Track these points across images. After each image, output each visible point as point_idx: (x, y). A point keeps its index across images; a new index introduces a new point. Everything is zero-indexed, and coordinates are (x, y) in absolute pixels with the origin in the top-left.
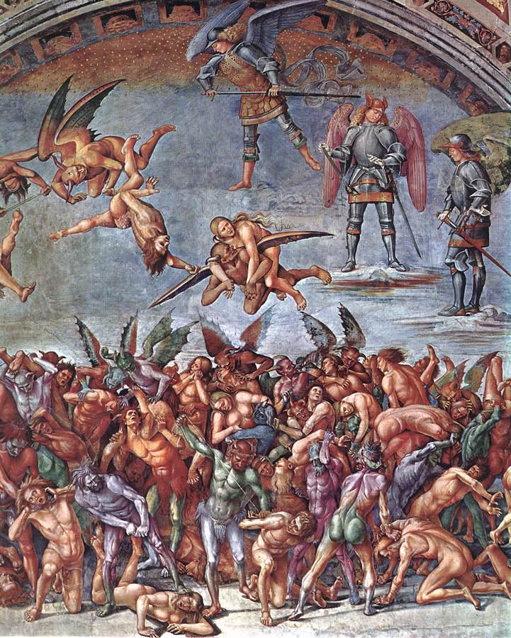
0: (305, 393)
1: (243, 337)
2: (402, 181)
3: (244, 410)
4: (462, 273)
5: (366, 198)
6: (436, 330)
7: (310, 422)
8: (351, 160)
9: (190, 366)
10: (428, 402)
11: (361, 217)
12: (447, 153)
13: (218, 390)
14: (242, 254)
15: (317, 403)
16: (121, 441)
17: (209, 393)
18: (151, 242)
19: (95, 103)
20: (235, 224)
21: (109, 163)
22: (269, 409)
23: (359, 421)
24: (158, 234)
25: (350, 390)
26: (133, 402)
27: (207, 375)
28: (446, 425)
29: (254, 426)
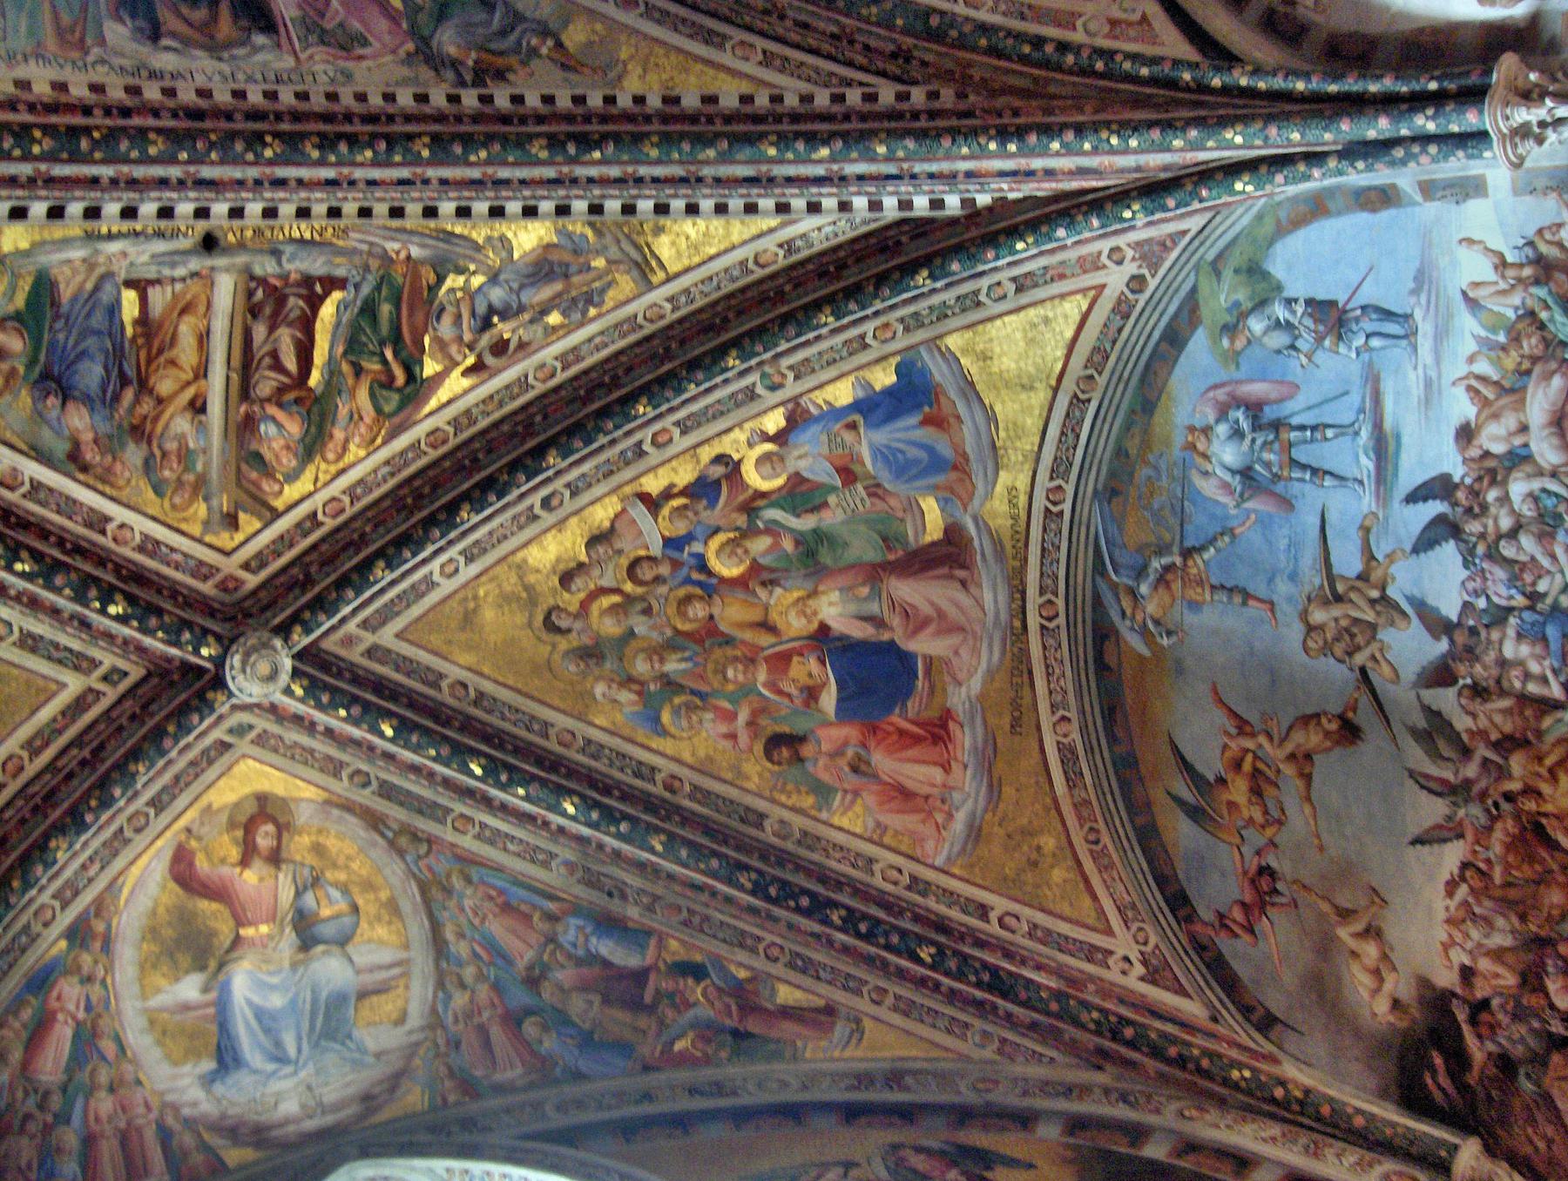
0: (1509, 562)
1: (1437, 638)
2: (1269, 413)
3: (1525, 650)
4: (1368, 336)
5: (1285, 458)
6: (1433, 374)
7: (1545, 562)
8: (1246, 473)
9: (1469, 713)
10: (1524, 389)
11: (1304, 467)
12: (1238, 353)
13: (1498, 682)
14: (1344, 623)
15: (1520, 548)
16: (1555, 822)
17: (1503, 693)
18: (1327, 734)
19: (1186, 766)
20: (1311, 629)
21: (1247, 766)
22: (1527, 615)
23: (1544, 490)
24: (1319, 724)
25: (1505, 499)
26: (1509, 797)
27: (1478, 691)
28: (1553, 365)
29: (1544, 639)
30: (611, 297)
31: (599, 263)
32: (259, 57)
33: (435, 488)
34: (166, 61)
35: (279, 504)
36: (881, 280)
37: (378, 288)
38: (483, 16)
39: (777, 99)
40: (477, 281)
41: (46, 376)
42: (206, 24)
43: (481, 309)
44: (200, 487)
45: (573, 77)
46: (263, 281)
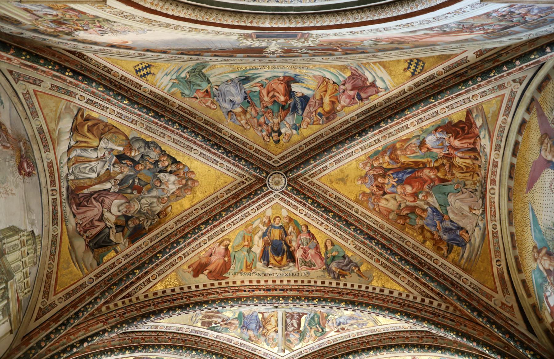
30: (368, 325)
31: (365, 319)
32: (290, 269)
33: (327, 353)
34: (269, 271)
35: (294, 349)
36: (430, 347)
37: (315, 315)
38: (342, 261)
39: (408, 296)
40: (336, 317)
41: (243, 326)
42: (280, 261)
43: (338, 322)
44: (277, 344)
45: (361, 278)
46: (288, 313)
